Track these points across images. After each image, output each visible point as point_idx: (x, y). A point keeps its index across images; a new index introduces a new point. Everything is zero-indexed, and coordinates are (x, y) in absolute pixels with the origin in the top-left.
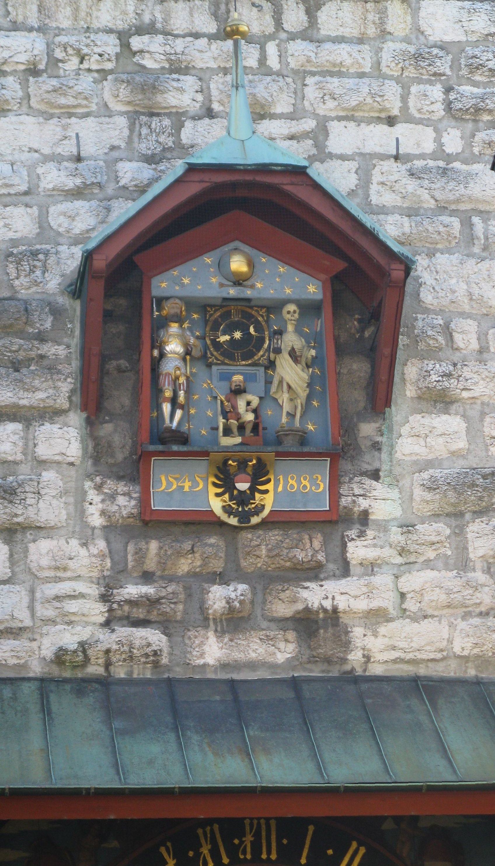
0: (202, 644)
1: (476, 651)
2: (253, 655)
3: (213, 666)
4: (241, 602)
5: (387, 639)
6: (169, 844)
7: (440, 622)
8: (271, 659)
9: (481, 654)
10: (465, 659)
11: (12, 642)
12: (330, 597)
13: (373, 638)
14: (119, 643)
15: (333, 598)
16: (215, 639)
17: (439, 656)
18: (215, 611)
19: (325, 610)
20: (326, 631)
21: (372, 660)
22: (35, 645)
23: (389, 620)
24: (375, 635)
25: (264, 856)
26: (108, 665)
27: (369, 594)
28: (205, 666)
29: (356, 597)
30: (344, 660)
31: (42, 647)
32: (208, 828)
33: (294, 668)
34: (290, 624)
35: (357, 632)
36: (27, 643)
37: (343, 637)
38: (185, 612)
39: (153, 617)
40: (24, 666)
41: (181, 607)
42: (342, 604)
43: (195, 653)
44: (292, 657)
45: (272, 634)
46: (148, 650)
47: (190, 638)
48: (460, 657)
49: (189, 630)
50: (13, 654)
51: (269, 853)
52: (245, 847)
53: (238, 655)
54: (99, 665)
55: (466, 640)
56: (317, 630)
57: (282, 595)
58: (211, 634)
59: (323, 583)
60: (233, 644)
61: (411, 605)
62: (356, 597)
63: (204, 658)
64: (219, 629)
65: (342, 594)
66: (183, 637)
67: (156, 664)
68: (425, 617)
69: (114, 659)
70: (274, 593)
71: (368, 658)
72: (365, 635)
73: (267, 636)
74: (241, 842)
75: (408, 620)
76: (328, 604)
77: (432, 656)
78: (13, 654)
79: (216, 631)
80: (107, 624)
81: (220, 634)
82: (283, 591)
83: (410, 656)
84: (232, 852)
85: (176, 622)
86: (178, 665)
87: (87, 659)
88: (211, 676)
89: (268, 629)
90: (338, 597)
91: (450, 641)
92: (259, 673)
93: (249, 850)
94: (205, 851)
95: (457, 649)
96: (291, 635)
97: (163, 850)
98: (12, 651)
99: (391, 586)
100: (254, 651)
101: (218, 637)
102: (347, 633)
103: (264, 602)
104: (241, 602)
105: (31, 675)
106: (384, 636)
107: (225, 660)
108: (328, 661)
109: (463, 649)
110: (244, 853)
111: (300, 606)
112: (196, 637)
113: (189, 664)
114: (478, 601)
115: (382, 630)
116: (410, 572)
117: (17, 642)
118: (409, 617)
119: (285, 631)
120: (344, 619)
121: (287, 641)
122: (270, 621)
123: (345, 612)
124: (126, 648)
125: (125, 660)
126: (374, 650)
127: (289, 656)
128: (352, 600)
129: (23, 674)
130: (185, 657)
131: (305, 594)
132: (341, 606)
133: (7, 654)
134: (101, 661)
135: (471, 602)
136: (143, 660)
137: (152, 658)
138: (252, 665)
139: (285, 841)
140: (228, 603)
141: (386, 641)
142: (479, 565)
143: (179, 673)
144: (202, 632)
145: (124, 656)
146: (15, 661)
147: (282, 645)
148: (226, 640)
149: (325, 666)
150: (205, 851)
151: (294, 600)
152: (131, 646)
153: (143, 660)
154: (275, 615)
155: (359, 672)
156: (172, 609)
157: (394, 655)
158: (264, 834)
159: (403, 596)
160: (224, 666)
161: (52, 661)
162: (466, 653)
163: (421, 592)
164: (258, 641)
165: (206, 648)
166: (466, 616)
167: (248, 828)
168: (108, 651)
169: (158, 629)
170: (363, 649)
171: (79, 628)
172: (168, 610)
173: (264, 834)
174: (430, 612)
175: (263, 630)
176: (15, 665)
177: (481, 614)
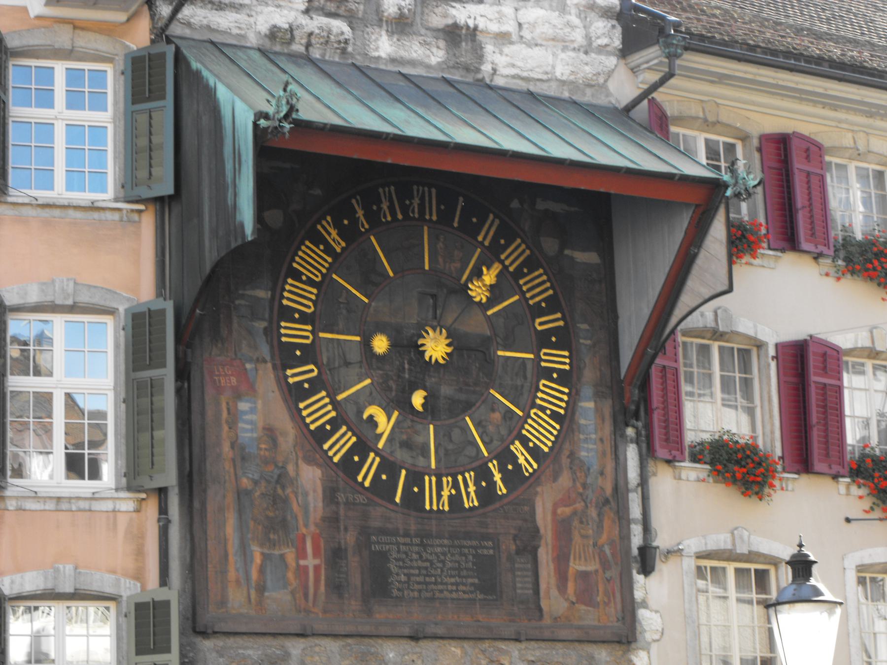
0: (377, 40)
1: (572, 78)
2: (414, 55)
3: (385, 59)
4: (409, 10)
5: (508, 58)
6: (358, 197)
7: (546, 50)
8: (427, 60)
9: (574, 80)
10: (563, 83)
11: (234, 15)
12: (473, 17)
13: (499, 55)
14: (321, 28)
15: (475, 19)
16: (387, 38)
17: (545, 77)
18: (389, 15)
19: (468, 27)
20: (467, 44)
21: (498, 73)
22: (252, 20)
23: (512, 43)
24: (501, 53)
25: (427, 217)
26: (308, 45)
27: (500, 20)
28: (379, 58)
29: (491, 20)
30: (478, 70)
31: (258, 23)
32: (387, 189)
33: (443, 70)
34: (441, 35)
35: (489, 48)
36: (246, 18)
37: (479, 52)
38: (365, 12)
39: (341, 11)
40: (243, 37)
41: (361, 7)
42: (482, 24)
43: (372, 46)
44: (443, 62)
45: (428, 40)
46: (342, 38)
47: (368, 34)
48: (557, 80)
49: (367, 27)
50: (236, 25)
51: (431, 215)
52: (414, 207)
53: (403, 53)
54: (301, 44)
55: (566, 67)
56: (460, 42)
57: (436, 10)
58: (384, 33)
59: (465, 5)
60: (400, 43)
61: (526, 34)
62: (491, 20)
63: (378, 51)
64: (390, 30)
65: (481, 16)
66: (363, 31)
67: (344, 51)
68: (536, 45)
69: (313, 41)
70: (430, 7)
71: (495, 70)
72: (494, 52)
73: (425, 41)
74: (411, 203)
75: (524, 45)
76: (471, 24)
77: (540, 76)
78: (236, 25)
79: (387, 31)
80: (307, 12)
81: (391, 33)
82: (437, 7)
83: (525, 74)
84: (405, 210)
85: (358, 18)
86: (359, 54)
87: (293, 38)
88: (382, 67)
89: (426, 35)
90: (478, 18)
91: (553, 67)
92: (418, 70)
93: (416, 210)
94: (385, 206)
95: (558, 74)
96: (442, 43)
97: (354, 201)
98: (236, 22)
99: (513, 16)
100: (415, 52)
101: (388, 35)
102: (482, 48)
103: (422, 13)
104: (409, 10)
105: (248, 45)
106: (507, 55)
107: (394, 55)
108: (467, 69)
109: (562, 74)
110: (413, 212)
111: (450, 21)
112: (372, 33)
113: (367, 54)
114: (573, 39)
115: (507, 50)
116: (526, 8)
117: (238, 16)
118: (525, 43)
119: (437, 39)
120: (480, 37)
121: (438, 47)
122: (427, 29)
123: (481, 32)
124: (325, 34)
125: (322, 44)
126: (500, 65)
127: (439, 60)
128: (488, 22)
129: (243, 43)
130: (365, 48)
131: (453, 12)
132: (481, 26)
133: (231, 25)
134: (304, 41)
135: (569, 38)
136: (336, 45)
137: (342, 45)
138: (413, 63)
139: (443, 207)
140: (399, 9)
141: (508, 59)
142: (574, 11)
143: (359, 61)
144: (377, 30)
145: (322, 40)
146: (238, 32)
147: (434, 50)
148: (395, 40)
149: (463, 73)
150: (385, 206)
151: (445, 16)
152: (329, 32)
153: (336, 45)
154: (430, 25)
155: (488, 81)
156: (356, 7)
157: (513, 71)
158: (427, 199)
159: (520, 25)
160: (393, 60)
161: (266, 35)
162: (564, 78)
163: (533, 25)
164: (418, 44)
165: (380, 43)
166: (565, 49)
167: (415, 193)
168: (311, 34)
169: (346, 22)
170: (492, 63)
171: (285, 12)
172: (354, 8)
173: (427, 199)
174: (539, 42)
175: (422, 35)
176: (237, 34)
177: (574, 49)
